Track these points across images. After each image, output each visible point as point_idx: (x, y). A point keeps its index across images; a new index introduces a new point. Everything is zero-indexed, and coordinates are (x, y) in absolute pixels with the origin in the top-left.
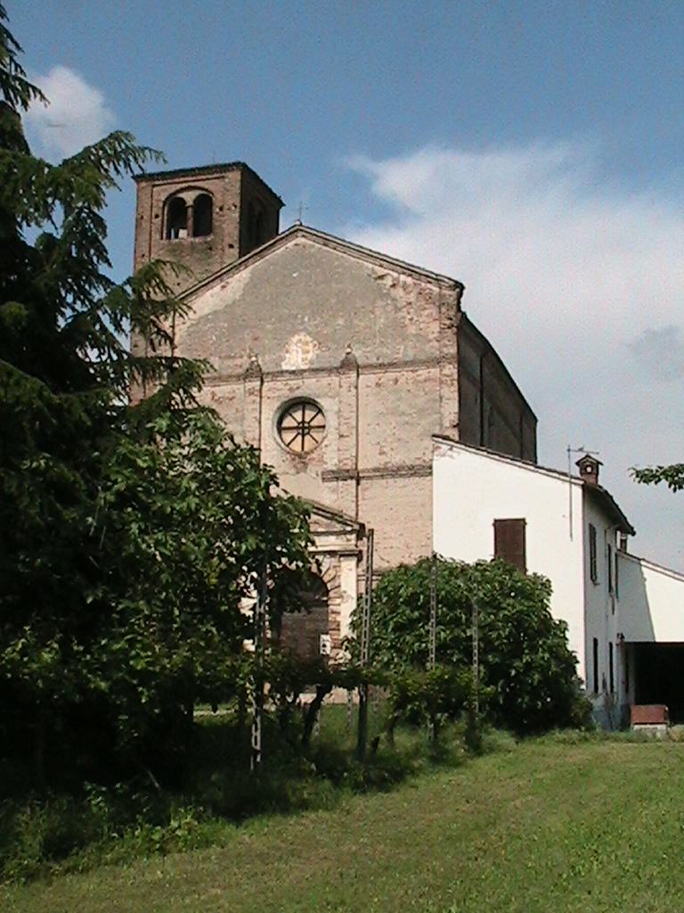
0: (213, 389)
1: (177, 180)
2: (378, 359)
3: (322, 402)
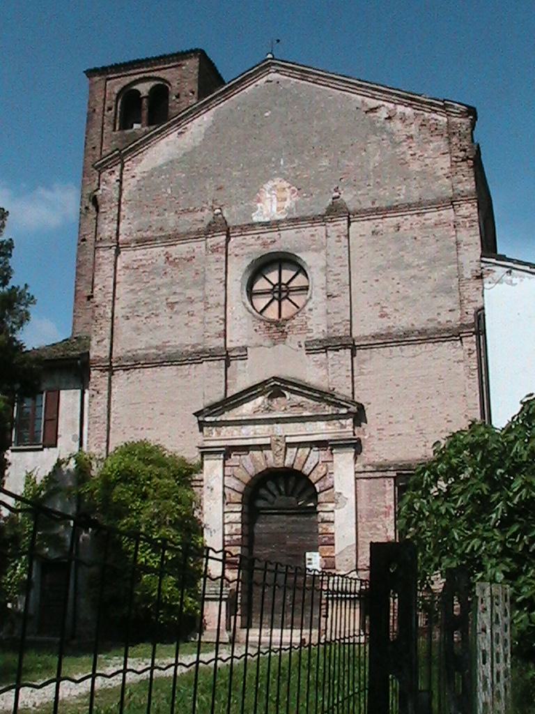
0: (168, 249)
1: (131, 72)
2: (373, 203)
3: (306, 258)
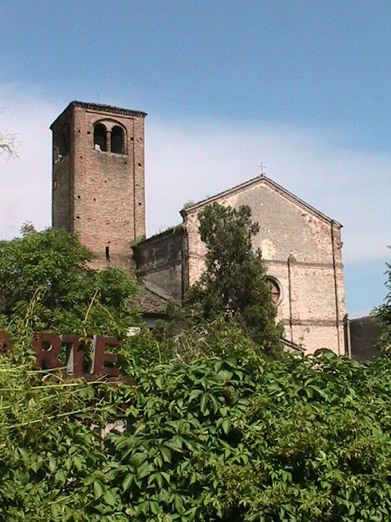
1: (102, 112)
